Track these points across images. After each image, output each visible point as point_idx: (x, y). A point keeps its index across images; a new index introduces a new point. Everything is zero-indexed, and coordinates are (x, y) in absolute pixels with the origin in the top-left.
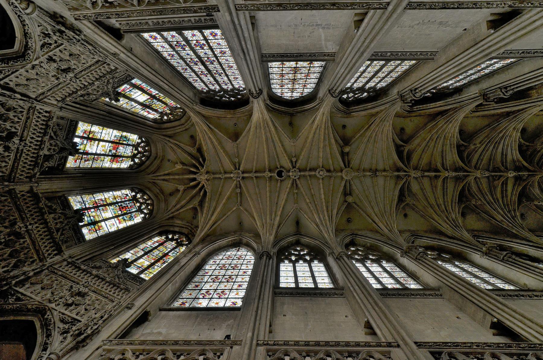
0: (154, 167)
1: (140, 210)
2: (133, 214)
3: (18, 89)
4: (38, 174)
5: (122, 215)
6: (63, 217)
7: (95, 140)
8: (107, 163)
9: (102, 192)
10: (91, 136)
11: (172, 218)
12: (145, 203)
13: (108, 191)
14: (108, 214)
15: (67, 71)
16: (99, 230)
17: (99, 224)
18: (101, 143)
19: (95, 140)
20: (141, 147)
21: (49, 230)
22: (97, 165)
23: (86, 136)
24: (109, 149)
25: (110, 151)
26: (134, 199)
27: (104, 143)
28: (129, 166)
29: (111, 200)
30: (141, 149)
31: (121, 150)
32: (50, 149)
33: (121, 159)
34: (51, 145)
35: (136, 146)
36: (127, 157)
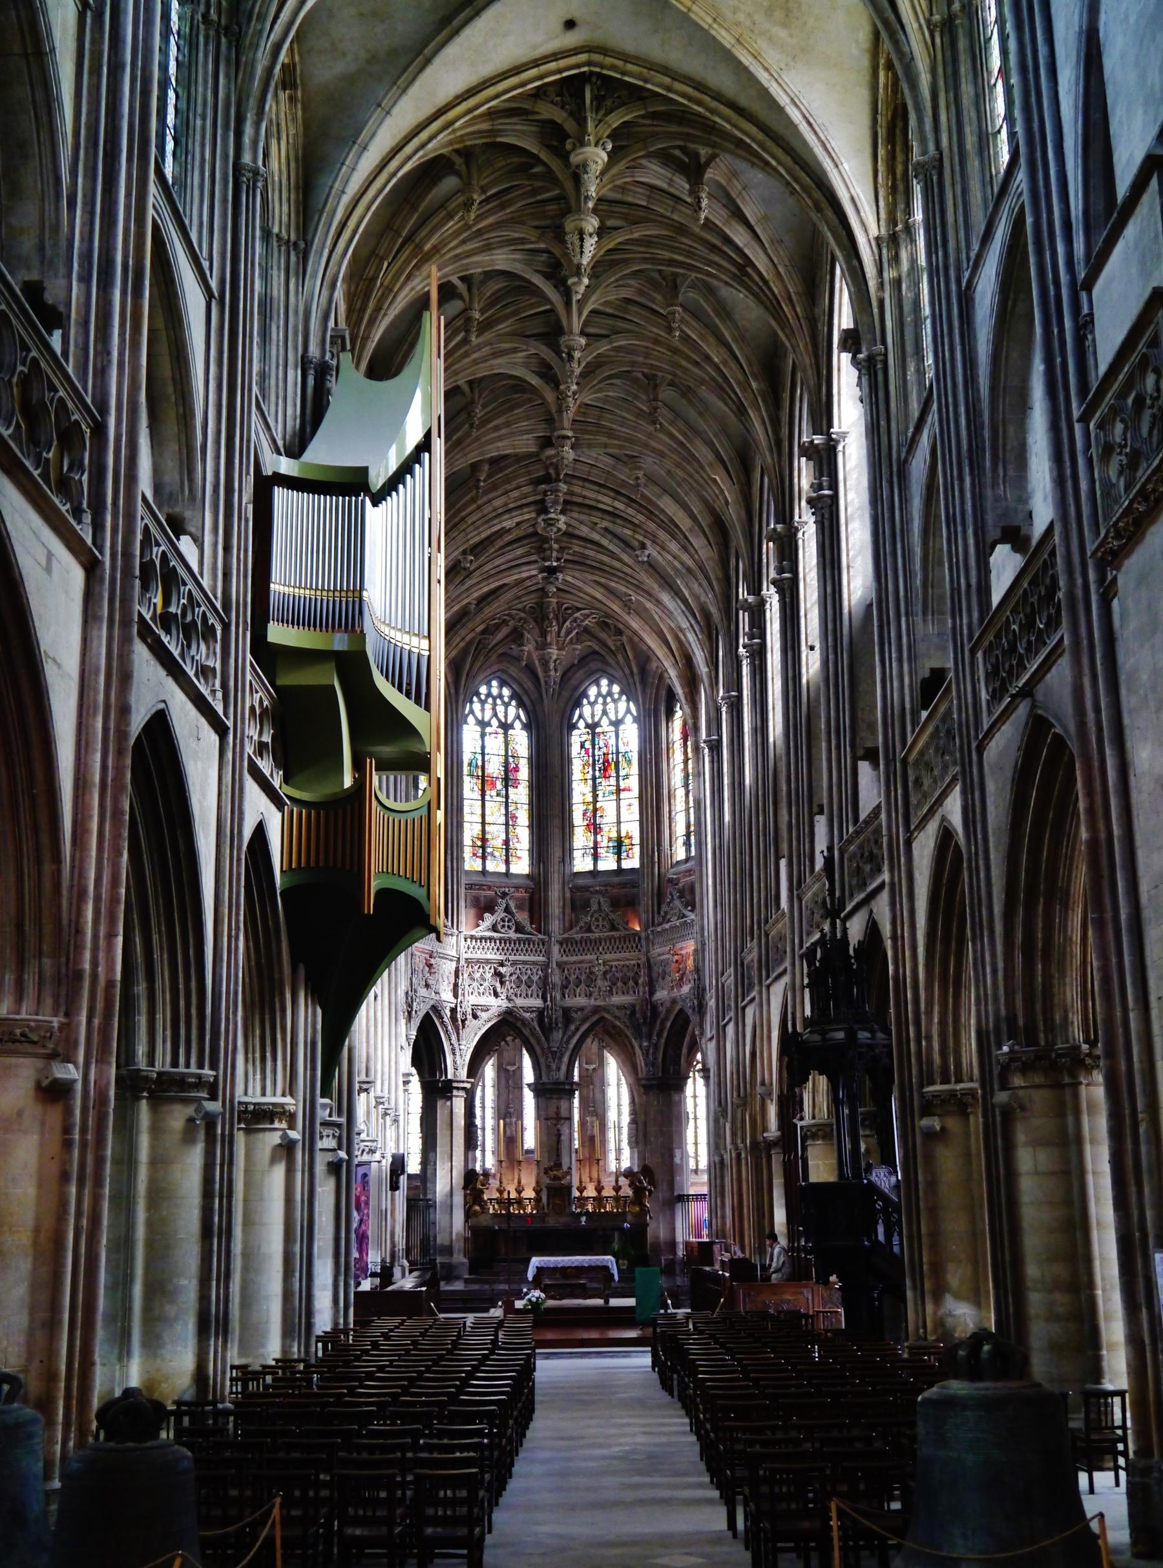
0: (526, 679)
1: (617, 724)
2: (622, 749)
3: (452, 980)
4: (540, 936)
5: (618, 777)
6: (596, 915)
7: (484, 831)
8: (521, 794)
9: (571, 806)
10: (479, 843)
11: (643, 671)
12: (605, 697)
13: (570, 790)
14: (608, 806)
15: (430, 966)
16: (631, 838)
17: (623, 834)
18: (488, 819)
19: (484, 831)
20: (483, 710)
21: (610, 938)
22: (523, 817)
23: (481, 851)
24: (496, 799)
25: (498, 795)
26: (592, 727)
27: (487, 812)
28: (524, 733)
29: (588, 789)
30: (488, 707)
31: (494, 767)
32: (509, 927)
33: (511, 760)
34: (503, 926)
35: (483, 724)
36: (507, 744)
